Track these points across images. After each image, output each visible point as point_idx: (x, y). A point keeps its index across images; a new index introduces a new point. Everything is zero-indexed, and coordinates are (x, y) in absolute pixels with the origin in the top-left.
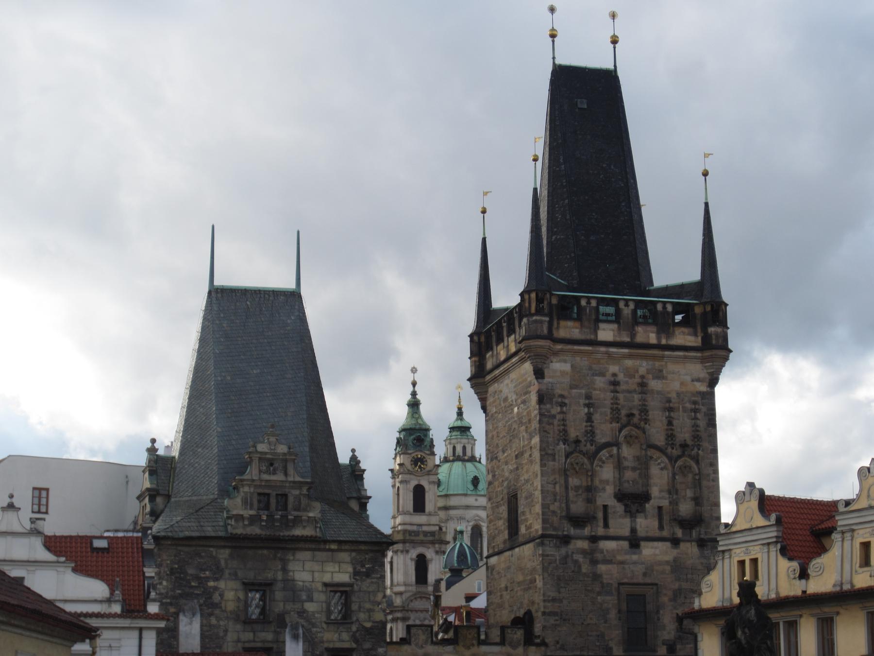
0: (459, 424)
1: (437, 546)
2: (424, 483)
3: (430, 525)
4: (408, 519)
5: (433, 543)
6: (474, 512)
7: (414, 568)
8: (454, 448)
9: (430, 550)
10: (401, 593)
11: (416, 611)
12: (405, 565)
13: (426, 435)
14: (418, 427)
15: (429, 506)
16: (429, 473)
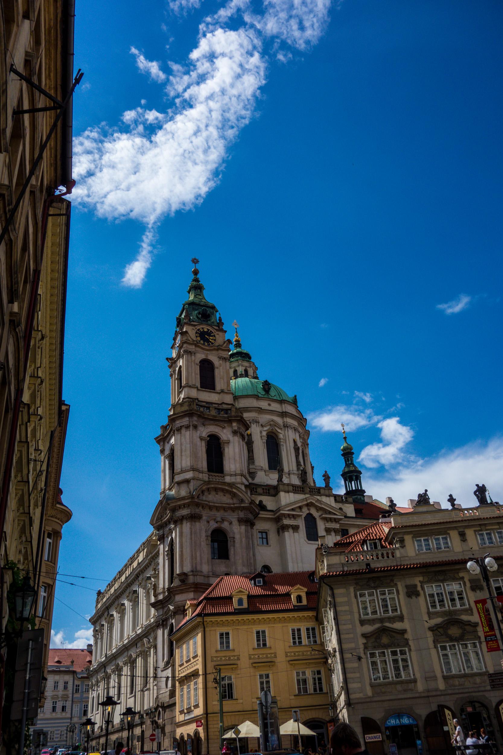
0: (239, 350)
1: (234, 424)
2: (213, 358)
3: (223, 403)
4: (194, 393)
5: (230, 421)
6: (268, 417)
7: (204, 449)
8: (235, 372)
9: (225, 431)
10: (187, 481)
11: (211, 508)
12: (192, 442)
13: (213, 314)
14: (202, 303)
15: (219, 385)
16: (219, 348)
